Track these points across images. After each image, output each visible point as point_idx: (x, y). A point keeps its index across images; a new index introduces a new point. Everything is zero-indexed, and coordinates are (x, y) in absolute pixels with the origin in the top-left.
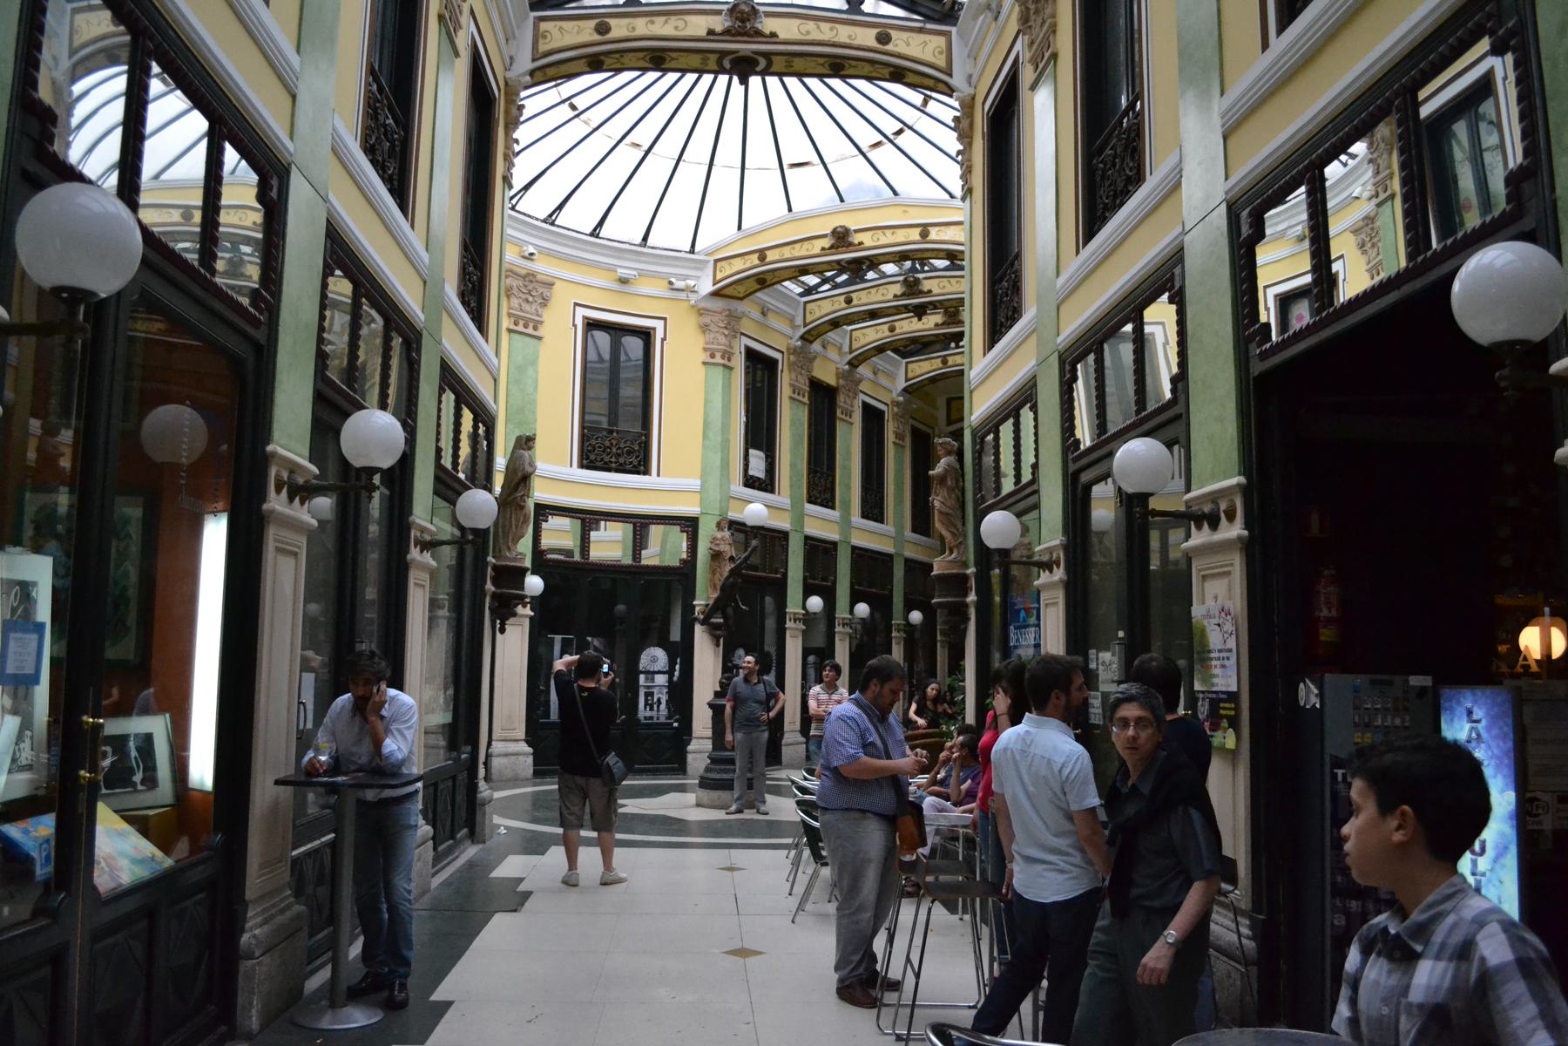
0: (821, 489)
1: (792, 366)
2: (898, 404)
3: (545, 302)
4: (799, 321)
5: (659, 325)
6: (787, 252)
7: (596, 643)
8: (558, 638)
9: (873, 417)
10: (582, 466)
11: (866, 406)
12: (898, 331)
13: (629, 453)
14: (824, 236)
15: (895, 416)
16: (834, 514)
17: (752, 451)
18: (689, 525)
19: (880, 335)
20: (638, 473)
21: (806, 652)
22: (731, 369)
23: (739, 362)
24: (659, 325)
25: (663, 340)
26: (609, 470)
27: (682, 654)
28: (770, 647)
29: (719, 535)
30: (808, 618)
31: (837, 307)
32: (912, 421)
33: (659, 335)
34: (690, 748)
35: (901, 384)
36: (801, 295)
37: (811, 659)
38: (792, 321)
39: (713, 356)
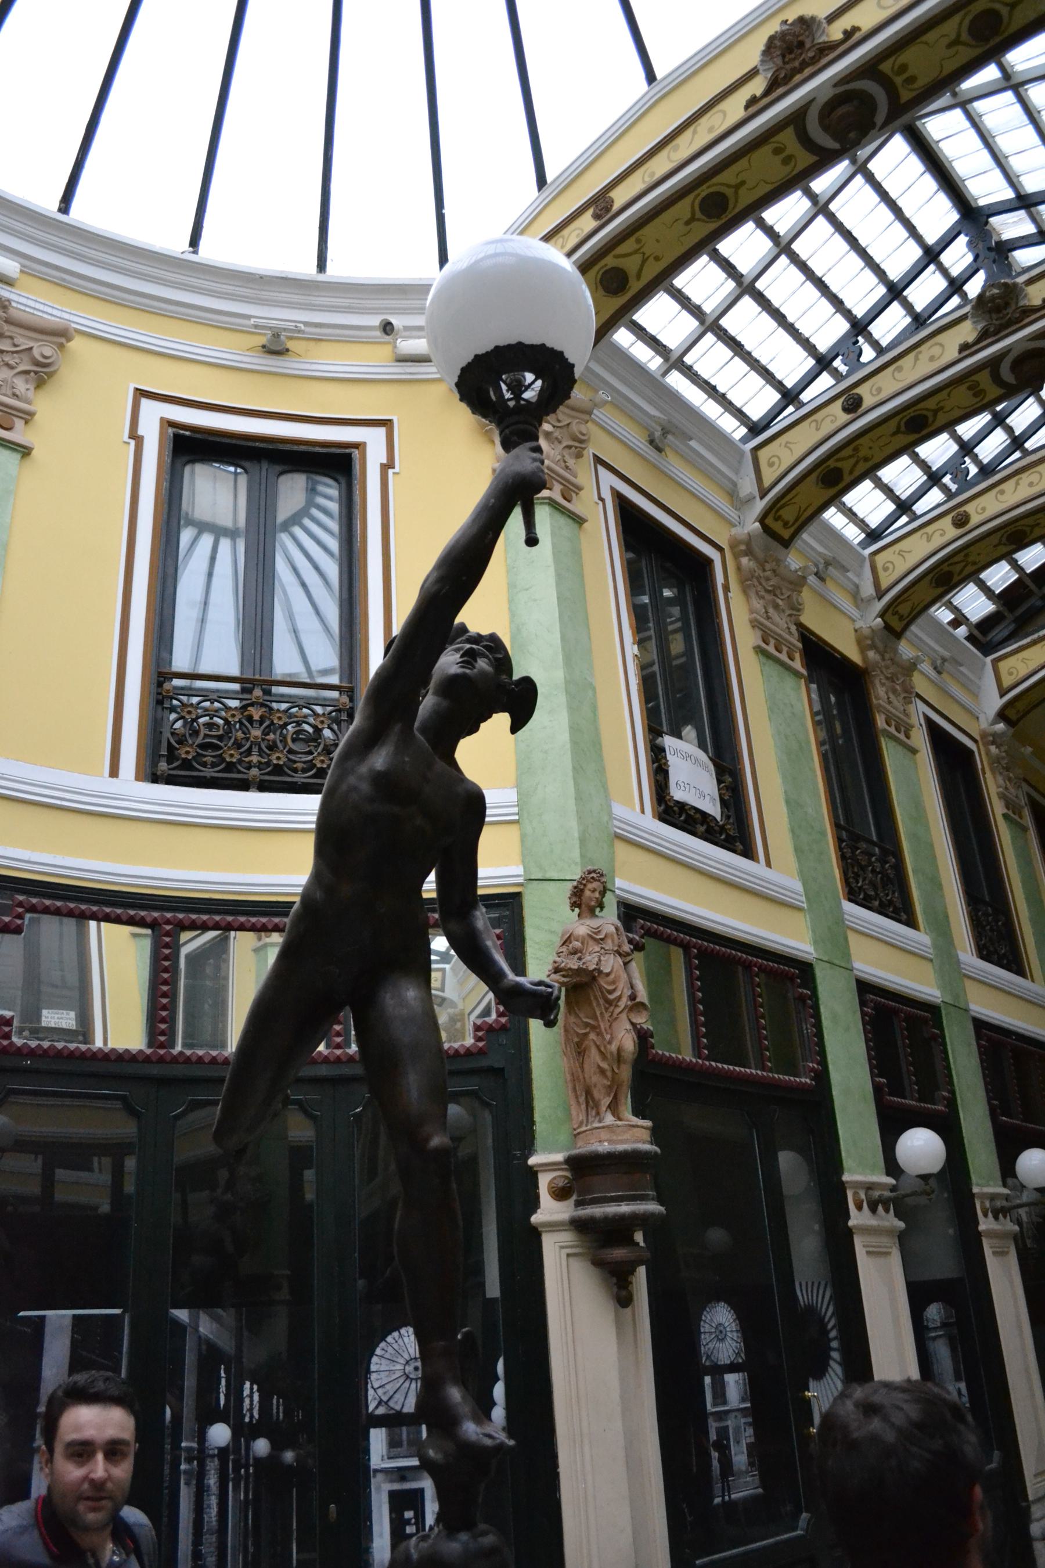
0: (873, 872)
1: (747, 582)
2: (995, 739)
3: (42, 374)
4: (748, 486)
6: (660, 165)
7: (206, 1327)
8: (59, 1320)
9: (952, 758)
10: (155, 779)
14: (752, 74)
15: (995, 761)
16: (921, 938)
17: (669, 742)
19: (938, 541)
21: (919, 1295)
22: (579, 520)
24: (374, 440)
25: (386, 467)
26: (243, 786)
27: (501, 1342)
28: (810, 1288)
30: (905, 1199)
31: (827, 428)
32: (1026, 787)
35: (992, 702)
36: (744, 440)
37: (934, 1312)
38: (732, 493)
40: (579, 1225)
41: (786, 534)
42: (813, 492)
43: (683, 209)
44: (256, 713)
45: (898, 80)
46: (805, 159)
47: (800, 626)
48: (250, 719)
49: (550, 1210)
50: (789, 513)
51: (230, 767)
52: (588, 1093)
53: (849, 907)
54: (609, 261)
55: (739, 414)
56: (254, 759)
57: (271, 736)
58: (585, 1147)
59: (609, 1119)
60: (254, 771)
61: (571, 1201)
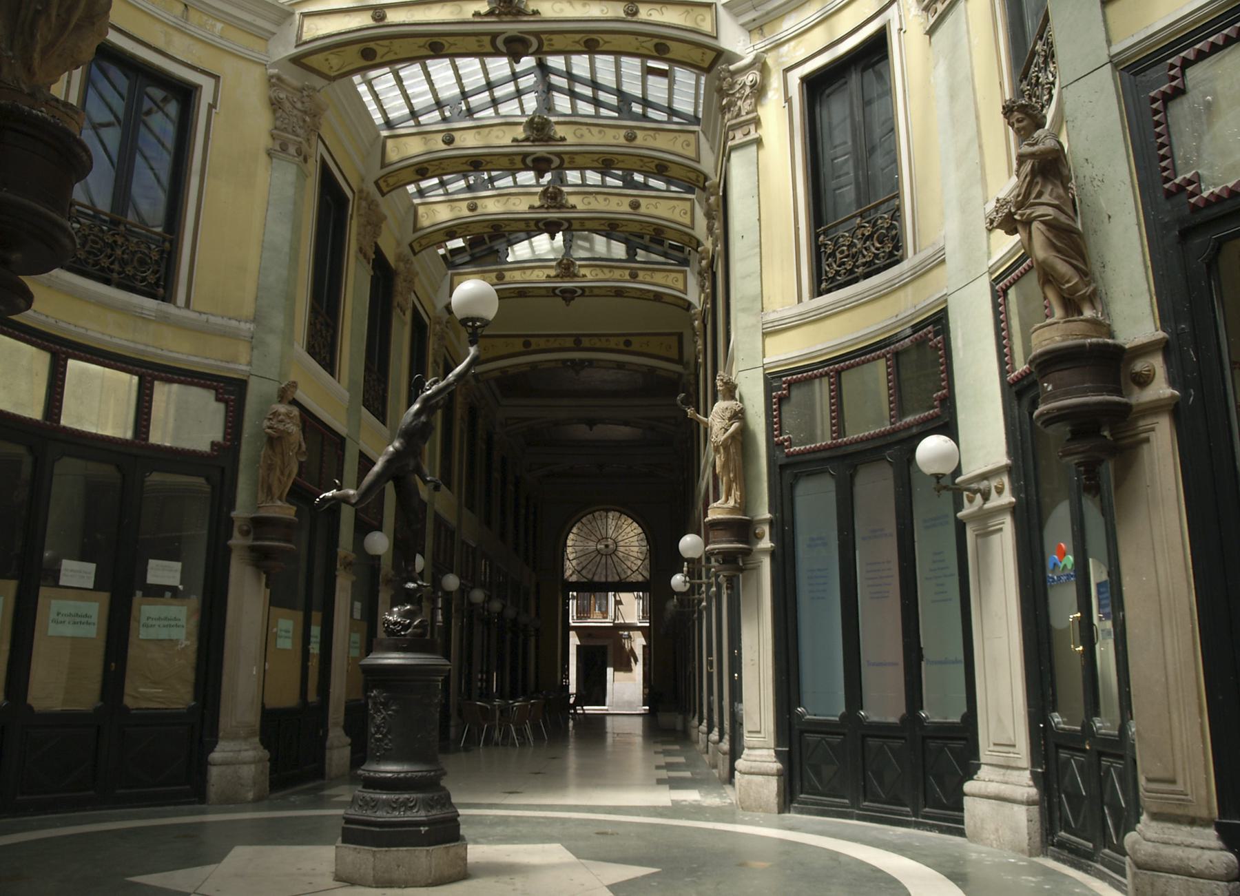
5: (207, 84)
11: (415, 312)
12: (479, 211)
13: (142, 262)
18: (231, 391)
20: (154, 297)
23: (313, 169)
25: (212, 107)
26: (107, 282)
29: (282, 408)
33: (206, 98)
34: (216, 756)
39: (284, 148)
40: (252, 549)
41: (385, 190)
42: (410, 174)
43: (422, 41)
44: (120, 240)
45: (546, 43)
46: (489, 49)
47: (376, 243)
48: (115, 242)
49: (237, 540)
50: (391, 181)
51: (102, 269)
52: (270, 489)
53: (363, 409)
54: (372, 45)
55: (384, 113)
56: (116, 267)
57: (125, 256)
58: (263, 513)
59: (279, 503)
60: (115, 275)
61: (251, 536)
